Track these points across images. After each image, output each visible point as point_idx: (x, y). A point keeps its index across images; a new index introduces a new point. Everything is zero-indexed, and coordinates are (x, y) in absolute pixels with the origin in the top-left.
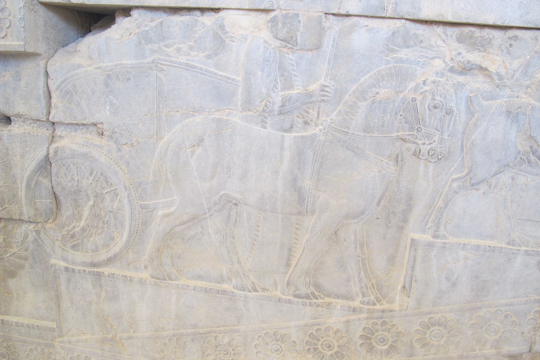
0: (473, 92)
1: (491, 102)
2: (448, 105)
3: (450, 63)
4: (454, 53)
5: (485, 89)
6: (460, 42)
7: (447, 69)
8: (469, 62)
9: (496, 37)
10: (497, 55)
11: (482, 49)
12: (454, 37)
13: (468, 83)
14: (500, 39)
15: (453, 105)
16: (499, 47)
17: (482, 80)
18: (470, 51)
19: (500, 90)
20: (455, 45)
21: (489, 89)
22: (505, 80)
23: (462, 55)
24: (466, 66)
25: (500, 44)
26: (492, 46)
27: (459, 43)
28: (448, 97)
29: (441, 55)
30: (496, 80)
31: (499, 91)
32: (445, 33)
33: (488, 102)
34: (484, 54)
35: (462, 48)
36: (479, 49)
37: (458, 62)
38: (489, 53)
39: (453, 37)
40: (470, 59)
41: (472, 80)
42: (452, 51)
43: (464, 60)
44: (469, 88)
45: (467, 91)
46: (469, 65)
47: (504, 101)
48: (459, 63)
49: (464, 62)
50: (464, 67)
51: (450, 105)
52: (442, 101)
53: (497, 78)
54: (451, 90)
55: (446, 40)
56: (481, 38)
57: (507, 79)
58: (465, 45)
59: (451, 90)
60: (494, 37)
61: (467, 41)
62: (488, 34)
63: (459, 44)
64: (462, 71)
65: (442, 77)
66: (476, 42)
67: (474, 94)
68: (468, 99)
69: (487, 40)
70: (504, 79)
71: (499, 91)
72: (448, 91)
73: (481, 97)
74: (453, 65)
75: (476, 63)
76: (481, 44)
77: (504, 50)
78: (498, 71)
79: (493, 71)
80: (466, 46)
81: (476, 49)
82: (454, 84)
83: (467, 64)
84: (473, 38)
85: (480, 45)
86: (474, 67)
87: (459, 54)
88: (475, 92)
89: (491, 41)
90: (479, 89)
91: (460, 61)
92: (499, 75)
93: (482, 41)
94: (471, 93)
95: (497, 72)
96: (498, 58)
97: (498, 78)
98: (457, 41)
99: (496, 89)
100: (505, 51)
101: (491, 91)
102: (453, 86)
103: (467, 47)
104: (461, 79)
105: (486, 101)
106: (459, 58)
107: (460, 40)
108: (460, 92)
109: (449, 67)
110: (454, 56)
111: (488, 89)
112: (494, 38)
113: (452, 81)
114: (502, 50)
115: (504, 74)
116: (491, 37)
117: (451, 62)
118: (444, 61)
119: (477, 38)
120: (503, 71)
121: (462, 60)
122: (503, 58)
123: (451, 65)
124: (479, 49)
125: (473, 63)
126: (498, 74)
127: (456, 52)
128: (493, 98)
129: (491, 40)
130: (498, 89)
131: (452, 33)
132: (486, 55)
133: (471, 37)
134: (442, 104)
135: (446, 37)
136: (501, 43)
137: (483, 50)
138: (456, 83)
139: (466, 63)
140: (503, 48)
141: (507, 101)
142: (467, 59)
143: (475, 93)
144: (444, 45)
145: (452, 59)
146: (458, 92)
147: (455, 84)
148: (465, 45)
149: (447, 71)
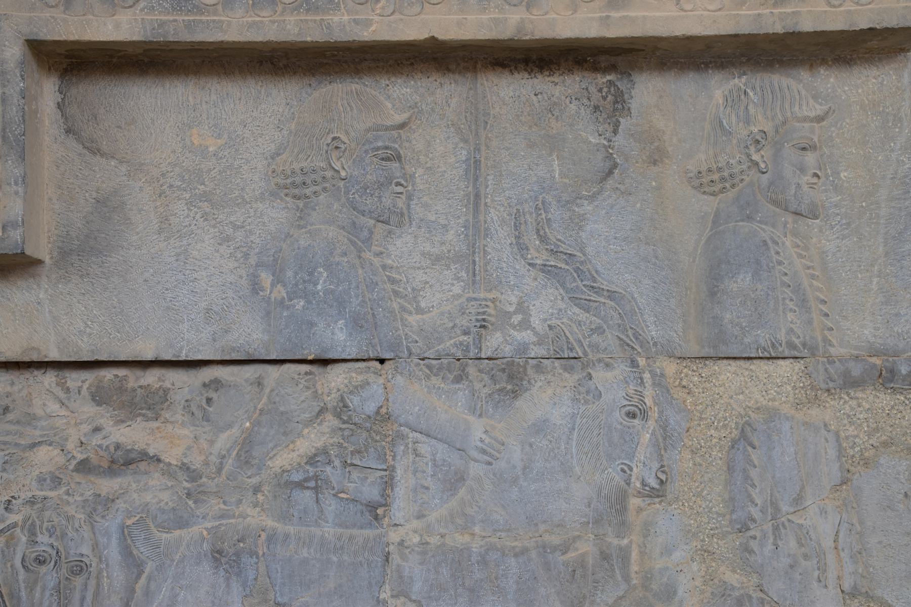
0: (132, 516)
1: (177, 533)
2: (72, 552)
3: (79, 451)
4: (86, 428)
5: (162, 504)
6: (99, 404)
7: (71, 467)
8: (118, 447)
9: (178, 385)
10: (183, 425)
11: (150, 414)
12: (84, 391)
13: (123, 493)
14: (187, 389)
15: (85, 550)
16: (184, 407)
17: (159, 483)
18: (123, 421)
19: (195, 502)
20: (89, 409)
21: (170, 504)
22: (204, 480)
23: (104, 433)
24: (115, 456)
25: (187, 401)
26: (169, 406)
27: (98, 405)
28: (71, 534)
29: (55, 436)
30: (184, 482)
31: (193, 506)
32: (62, 385)
33: (172, 535)
34: (155, 424)
35: (104, 417)
36: (144, 415)
37: (96, 448)
38: (166, 421)
39: (82, 393)
40: (122, 440)
41: (134, 485)
42: (81, 424)
43: (108, 443)
44: (125, 506)
45: (119, 513)
46: (119, 453)
47: (206, 529)
48: (99, 449)
49: (107, 447)
50: (111, 459)
51: (78, 552)
52: (55, 544)
53: (185, 477)
54: (78, 516)
55: (66, 402)
56: (142, 391)
57: (209, 478)
58: (111, 409)
59: (78, 516)
60: (173, 385)
61: (115, 398)
62: (159, 378)
63: (98, 408)
64: (109, 467)
65: (56, 487)
66: (133, 399)
67: (136, 519)
68: (123, 532)
69: (157, 393)
70: (201, 478)
71: (193, 506)
72: (69, 518)
73: (154, 523)
74: (85, 456)
75: (136, 447)
76: (145, 403)
77: (196, 413)
78: (185, 461)
79: (174, 462)
80: (114, 410)
81: (140, 414)
82: (86, 501)
83: (115, 450)
84: (126, 391)
85: (144, 405)
86: (133, 455)
87: (97, 429)
88: (138, 513)
89: (166, 396)
90: (147, 505)
91: (100, 446)
92: (188, 468)
93: (147, 396)
94: (129, 518)
95: (183, 464)
96: (185, 432)
97: (188, 476)
98: (93, 400)
99: (186, 503)
100: (199, 414)
101: (174, 509)
102: (83, 507)
103: (116, 412)
104: (107, 485)
105: (167, 532)
106: (97, 440)
107: (99, 397)
108: (103, 517)
109: (74, 462)
110: (85, 435)
111: (167, 503)
112: (173, 387)
113: (82, 495)
114: (193, 413)
115: (199, 466)
116: (167, 384)
117: (79, 449)
118: (63, 450)
119: (134, 390)
120: (196, 461)
121: (105, 443)
122: (196, 430)
123: (80, 457)
124: (144, 415)
125: (129, 447)
126: (185, 467)
127: (90, 427)
128: (182, 524)
129: (166, 391)
130: (190, 503)
131: (80, 384)
132: (158, 428)
133: (122, 390)
134: (55, 552)
135: (66, 393)
136: (189, 397)
137: (153, 415)
138: (91, 498)
139: (112, 449)
140: (194, 409)
141: (213, 527)
142: (114, 440)
143: (139, 516)
144: (63, 412)
145: (82, 443)
146: (98, 519)
147: (87, 500)
148: (111, 409)
149: (73, 471)
